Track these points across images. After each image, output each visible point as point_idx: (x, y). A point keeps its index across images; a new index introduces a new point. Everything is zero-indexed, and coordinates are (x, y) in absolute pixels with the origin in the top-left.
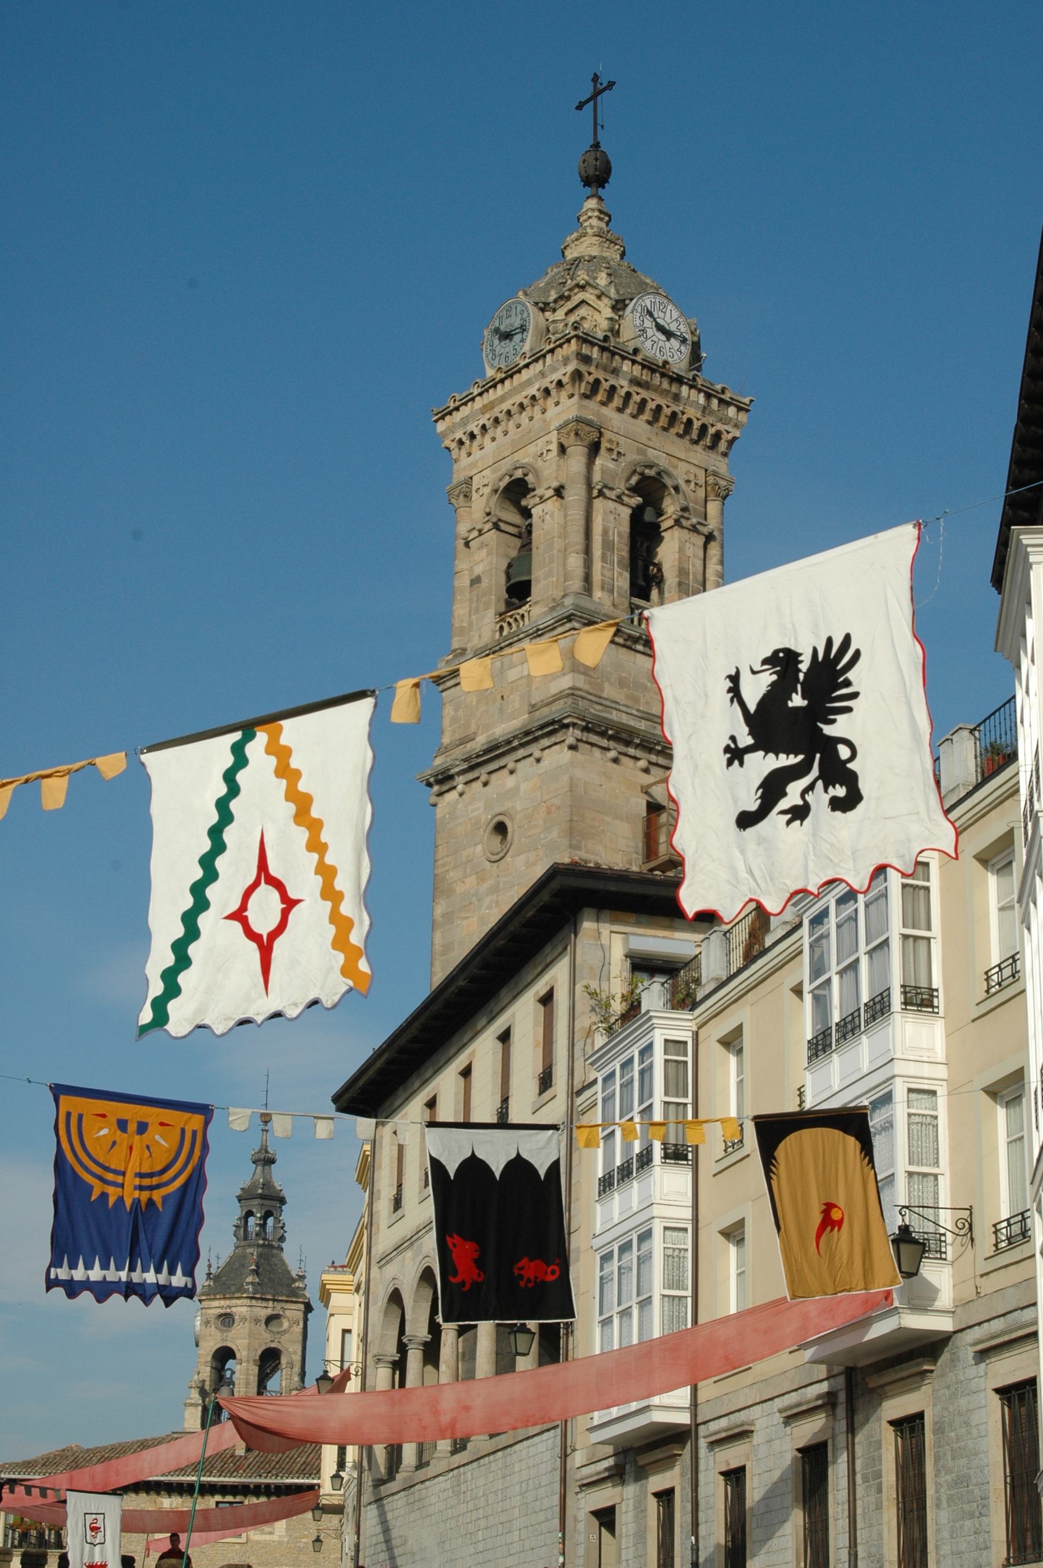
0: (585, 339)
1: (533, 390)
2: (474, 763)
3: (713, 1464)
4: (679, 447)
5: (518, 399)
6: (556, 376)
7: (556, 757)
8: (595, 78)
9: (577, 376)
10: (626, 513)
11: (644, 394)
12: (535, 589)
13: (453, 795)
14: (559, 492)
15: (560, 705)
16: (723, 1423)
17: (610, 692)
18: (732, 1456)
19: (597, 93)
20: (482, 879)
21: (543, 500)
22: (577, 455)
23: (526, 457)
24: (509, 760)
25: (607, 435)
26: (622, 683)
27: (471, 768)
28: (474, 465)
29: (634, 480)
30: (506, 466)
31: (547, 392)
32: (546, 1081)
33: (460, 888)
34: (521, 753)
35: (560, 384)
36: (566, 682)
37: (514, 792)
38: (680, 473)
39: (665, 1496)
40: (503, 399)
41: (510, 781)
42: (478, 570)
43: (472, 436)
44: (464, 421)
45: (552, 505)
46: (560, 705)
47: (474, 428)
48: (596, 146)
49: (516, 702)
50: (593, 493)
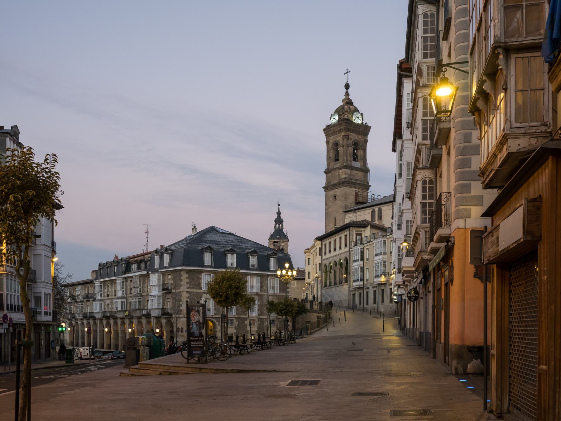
3: (365, 291)
18: (367, 290)
22: (345, 140)
23: (338, 139)
30: (335, 140)
32: (346, 245)
39: (360, 293)
45: (342, 148)
49: (337, 178)
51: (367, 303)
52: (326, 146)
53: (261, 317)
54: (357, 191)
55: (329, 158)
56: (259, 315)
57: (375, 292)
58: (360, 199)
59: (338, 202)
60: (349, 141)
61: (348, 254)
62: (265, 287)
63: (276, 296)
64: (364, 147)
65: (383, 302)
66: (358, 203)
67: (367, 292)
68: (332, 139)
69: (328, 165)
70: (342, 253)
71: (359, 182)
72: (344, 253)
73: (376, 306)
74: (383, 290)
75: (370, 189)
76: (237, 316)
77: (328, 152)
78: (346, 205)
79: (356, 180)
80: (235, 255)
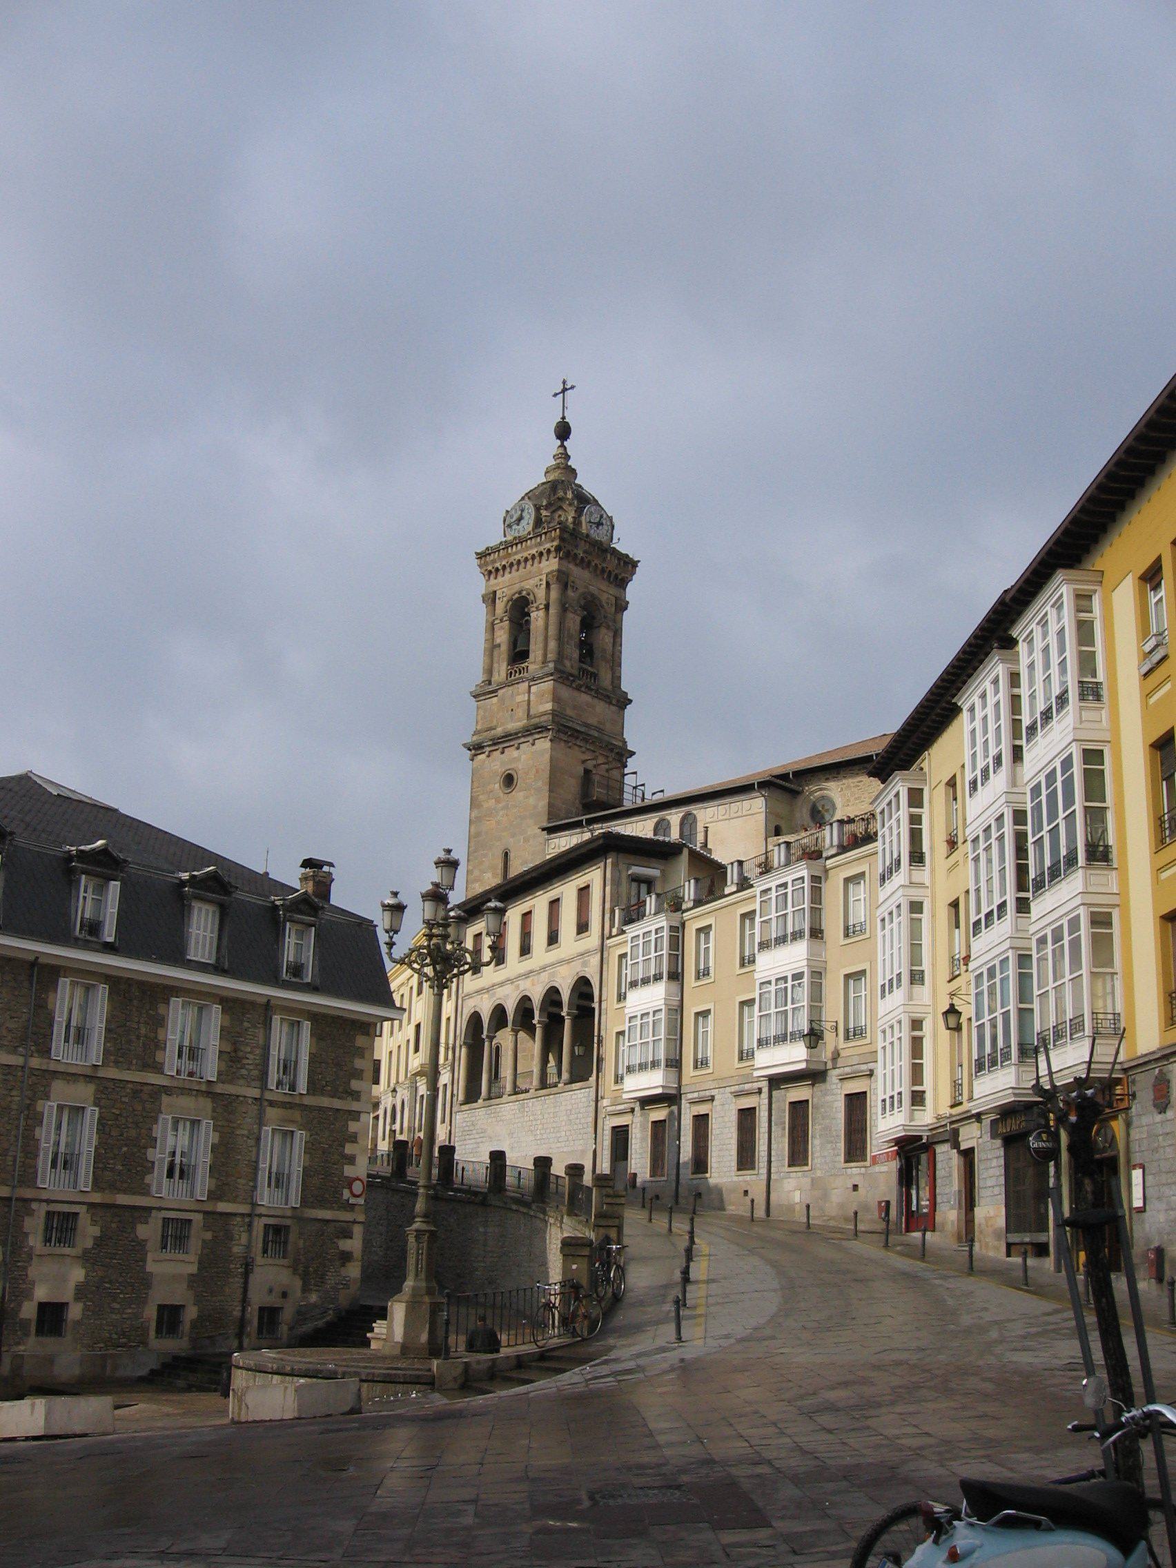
0: (564, 528)
1: (534, 551)
2: (496, 742)
3: (688, 1114)
4: (604, 586)
5: (525, 554)
6: (548, 546)
7: (544, 745)
8: (564, 382)
9: (558, 549)
10: (578, 619)
11: (590, 558)
12: (532, 655)
13: (483, 756)
14: (547, 607)
15: (545, 718)
16: (696, 1095)
17: (569, 712)
19: (564, 390)
20: (498, 801)
21: (538, 609)
23: (529, 585)
24: (515, 742)
25: (572, 578)
26: (575, 707)
27: (494, 744)
28: (498, 584)
29: (582, 603)
30: (516, 588)
31: (541, 554)
32: (582, 927)
33: (486, 805)
34: (523, 740)
35: (549, 551)
36: (549, 706)
37: (518, 759)
38: (604, 597)
40: (516, 553)
41: (515, 753)
42: (498, 641)
43: (497, 570)
44: (494, 561)
46: (545, 718)
47: (498, 565)
48: (564, 418)
49: (521, 713)
50: (564, 609)
51: (700, 1164)
52: (483, 609)
53: (223, 1207)
54: (590, 765)
55: (492, 648)
56: (214, 1196)
57: (747, 1117)
58: (598, 793)
59: (518, 795)
60: (570, 593)
61: (595, 960)
62: (252, 1059)
63: (304, 1107)
64: (615, 621)
65: (798, 1155)
66: (588, 806)
67: (701, 1122)
68: (507, 585)
69: (489, 671)
70: (561, 962)
71: (596, 734)
72: (568, 961)
73: (754, 1180)
74: (799, 1109)
75: (632, 764)
76: (97, 1198)
77: (491, 628)
78: (550, 805)
79: (586, 725)
80: (115, 886)
